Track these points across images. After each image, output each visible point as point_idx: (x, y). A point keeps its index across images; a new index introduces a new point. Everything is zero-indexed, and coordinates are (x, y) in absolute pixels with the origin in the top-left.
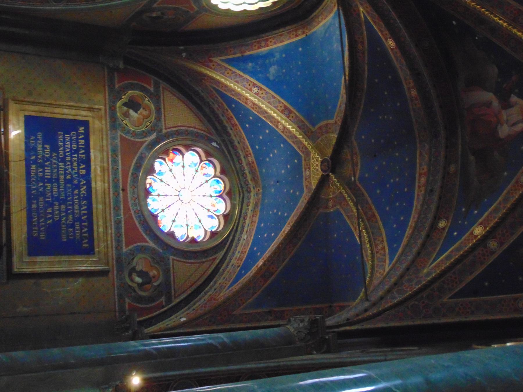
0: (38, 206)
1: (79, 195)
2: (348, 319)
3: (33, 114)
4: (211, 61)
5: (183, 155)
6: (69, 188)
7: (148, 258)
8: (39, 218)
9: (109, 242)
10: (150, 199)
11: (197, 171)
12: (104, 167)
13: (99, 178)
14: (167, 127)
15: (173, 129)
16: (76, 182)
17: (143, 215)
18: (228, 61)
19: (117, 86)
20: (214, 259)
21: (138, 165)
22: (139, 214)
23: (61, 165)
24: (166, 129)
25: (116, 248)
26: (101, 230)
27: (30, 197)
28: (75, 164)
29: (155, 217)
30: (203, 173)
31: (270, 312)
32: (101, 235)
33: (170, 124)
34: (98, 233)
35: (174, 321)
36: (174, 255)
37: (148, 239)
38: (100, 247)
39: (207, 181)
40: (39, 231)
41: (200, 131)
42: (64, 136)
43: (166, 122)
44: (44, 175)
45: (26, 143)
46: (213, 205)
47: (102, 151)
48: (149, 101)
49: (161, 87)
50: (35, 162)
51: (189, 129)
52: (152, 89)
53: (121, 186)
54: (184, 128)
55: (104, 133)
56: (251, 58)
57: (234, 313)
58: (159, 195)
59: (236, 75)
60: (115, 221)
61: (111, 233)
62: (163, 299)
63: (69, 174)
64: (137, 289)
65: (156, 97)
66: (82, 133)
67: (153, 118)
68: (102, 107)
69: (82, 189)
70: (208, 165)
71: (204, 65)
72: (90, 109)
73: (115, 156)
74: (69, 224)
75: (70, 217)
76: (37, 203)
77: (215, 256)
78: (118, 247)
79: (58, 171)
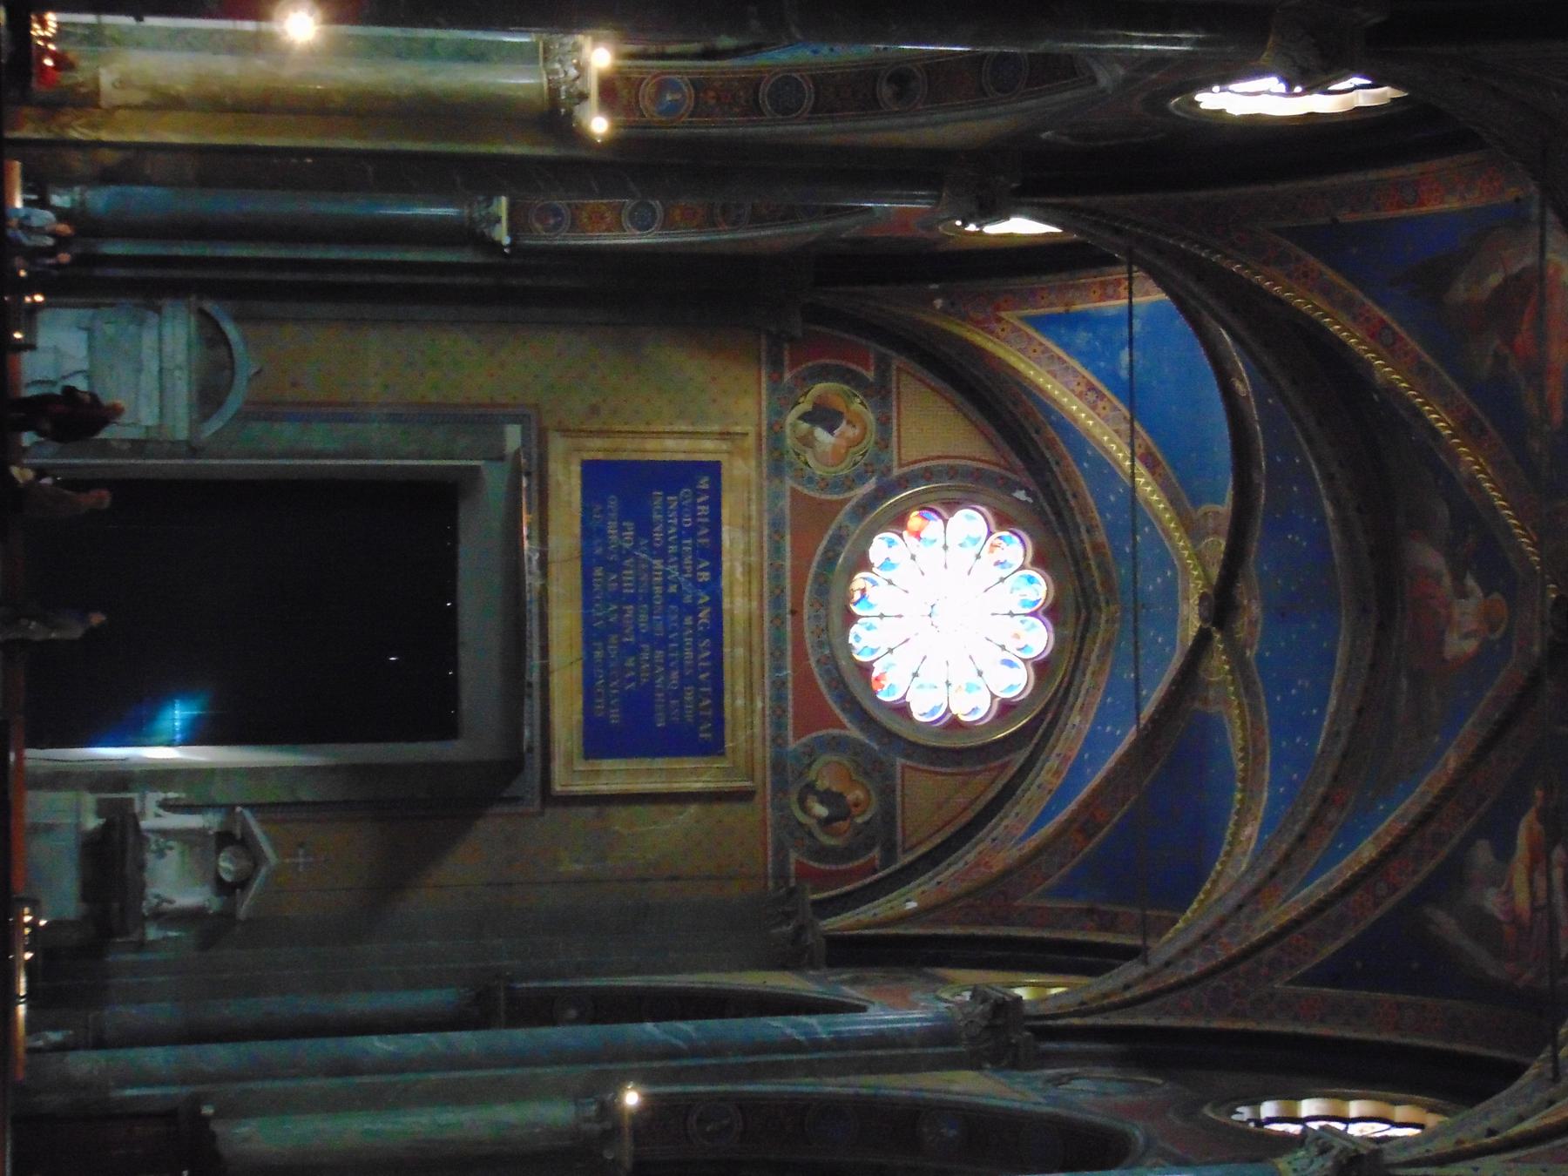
0: (607, 654)
1: (694, 627)
2: (1083, 1003)
3: (600, 456)
4: (999, 320)
5: (945, 522)
6: (673, 612)
7: (846, 762)
8: (608, 680)
9: (757, 730)
10: (861, 624)
11: (978, 557)
12: (750, 565)
13: (739, 590)
14: (903, 462)
15: (917, 466)
16: (688, 599)
17: (837, 668)
18: (1038, 323)
19: (787, 376)
20: (1004, 767)
21: (831, 554)
22: (829, 666)
23: (658, 563)
24: (901, 466)
25: (774, 740)
26: (740, 702)
27: (592, 634)
28: (688, 560)
29: (865, 669)
30: (995, 560)
31: (1090, 912)
32: (740, 713)
33: (911, 453)
34: (734, 710)
35: (892, 908)
36: (908, 757)
37: (845, 721)
38: (736, 738)
39: (1002, 580)
40: (608, 705)
41: (986, 466)
42: (665, 500)
43: (903, 451)
44: (621, 588)
45: (584, 521)
46: (1017, 636)
47: (746, 529)
48: (862, 403)
49: (894, 367)
50: (602, 561)
51: (958, 462)
52: (870, 375)
53: (789, 605)
54: (946, 462)
55: (753, 488)
56: (1084, 319)
57: (1019, 902)
58: (882, 616)
59: (1053, 358)
60: (773, 683)
61: (763, 708)
62: (876, 853)
63: (674, 583)
64: (817, 831)
65: (880, 394)
66: (704, 491)
67: (872, 438)
68: (751, 429)
69: (701, 615)
70: (1007, 540)
71: (983, 329)
72: (724, 435)
73: (777, 538)
74: (670, 690)
75: (675, 674)
76: (605, 648)
77: (1007, 759)
78: (778, 740)
79: (651, 577)
